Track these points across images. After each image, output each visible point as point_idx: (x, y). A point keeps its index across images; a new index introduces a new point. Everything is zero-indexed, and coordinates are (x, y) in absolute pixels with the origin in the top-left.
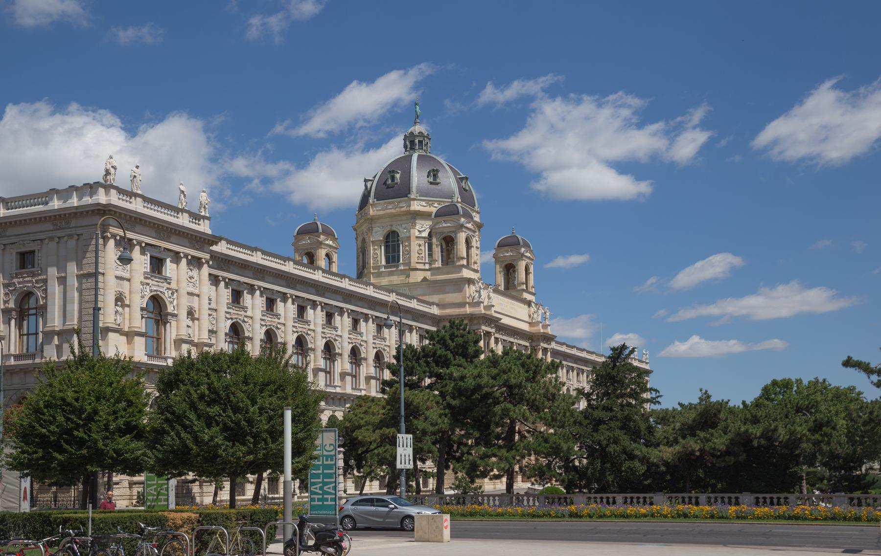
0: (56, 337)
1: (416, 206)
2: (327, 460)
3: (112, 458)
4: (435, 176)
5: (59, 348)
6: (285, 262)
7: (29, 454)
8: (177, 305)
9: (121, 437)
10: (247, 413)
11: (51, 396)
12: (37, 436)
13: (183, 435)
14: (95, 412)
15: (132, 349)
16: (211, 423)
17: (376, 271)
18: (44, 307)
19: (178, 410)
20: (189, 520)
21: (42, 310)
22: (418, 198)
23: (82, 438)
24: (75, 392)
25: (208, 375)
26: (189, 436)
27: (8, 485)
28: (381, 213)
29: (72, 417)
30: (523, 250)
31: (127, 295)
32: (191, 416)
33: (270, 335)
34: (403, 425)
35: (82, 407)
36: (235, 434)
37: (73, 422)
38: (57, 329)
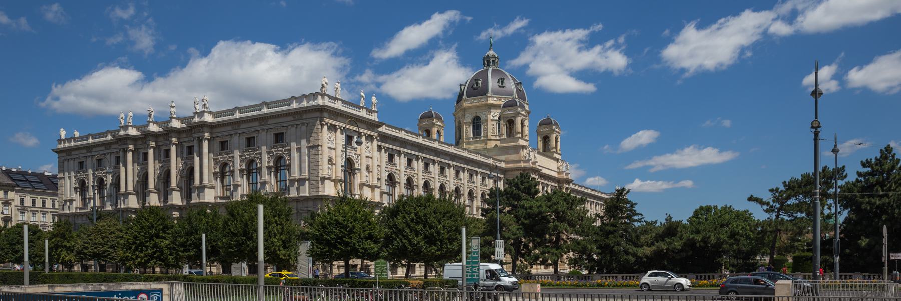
0: (296, 182)
1: (491, 101)
2: (474, 254)
3: (362, 253)
4: (502, 82)
5: (298, 189)
6: (434, 142)
7: (321, 249)
8: (361, 163)
9: (366, 241)
10: (437, 229)
11: (330, 218)
12: (324, 240)
13: (404, 240)
14: (354, 227)
15: (374, 195)
16: (418, 235)
17: (467, 141)
18: (289, 165)
19: (401, 226)
20: (419, 284)
21: (288, 167)
22: (492, 96)
23: (348, 241)
24: (342, 216)
25: (415, 209)
26: (407, 241)
27: (303, 266)
28: (470, 105)
29: (343, 230)
30: (554, 127)
31: (334, 158)
32: (407, 231)
33: (442, 187)
34: (498, 235)
35: (347, 224)
36: (431, 240)
37: (344, 233)
38: (297, 178)
